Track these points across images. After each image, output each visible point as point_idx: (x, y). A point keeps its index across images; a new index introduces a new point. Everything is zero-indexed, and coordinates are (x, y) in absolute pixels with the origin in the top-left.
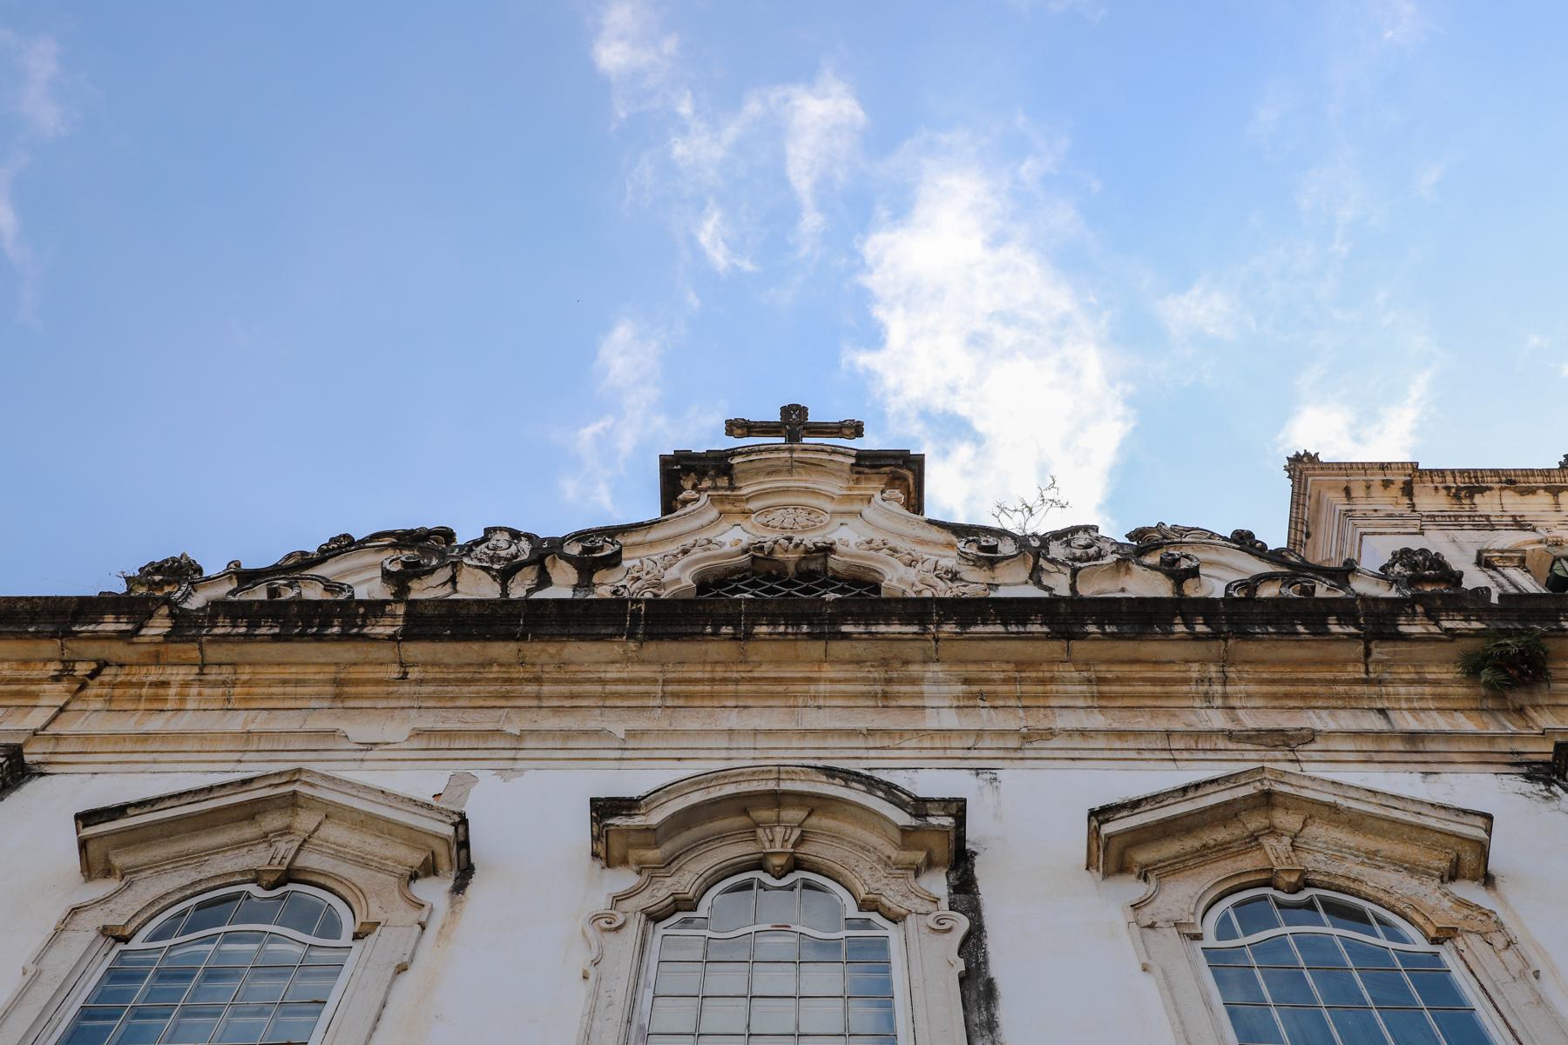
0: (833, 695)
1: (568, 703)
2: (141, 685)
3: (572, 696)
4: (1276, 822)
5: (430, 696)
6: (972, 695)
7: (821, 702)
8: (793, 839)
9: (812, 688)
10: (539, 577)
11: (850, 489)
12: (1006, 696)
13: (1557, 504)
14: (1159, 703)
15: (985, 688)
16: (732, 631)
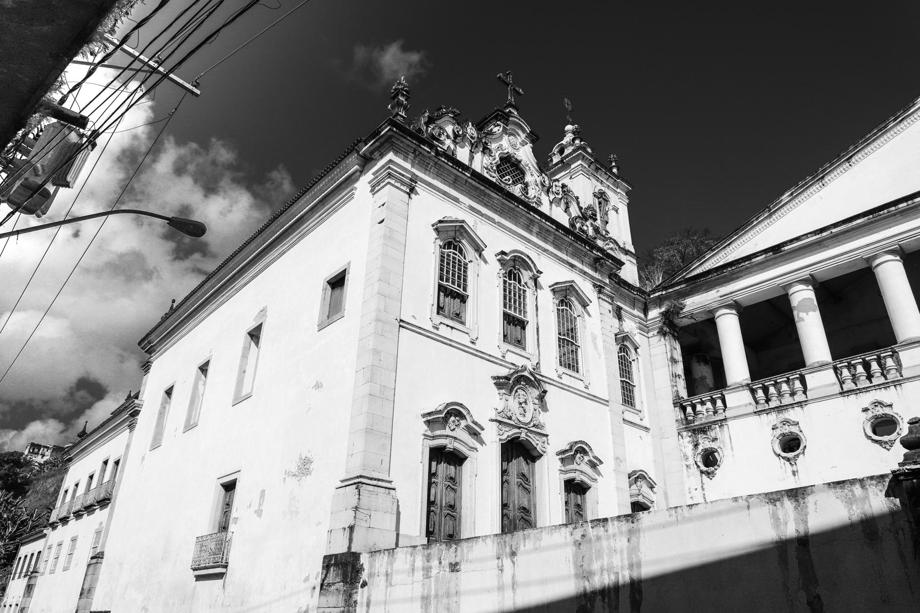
3: (488, 202)
5: (467, 190)
13: (608, 179)
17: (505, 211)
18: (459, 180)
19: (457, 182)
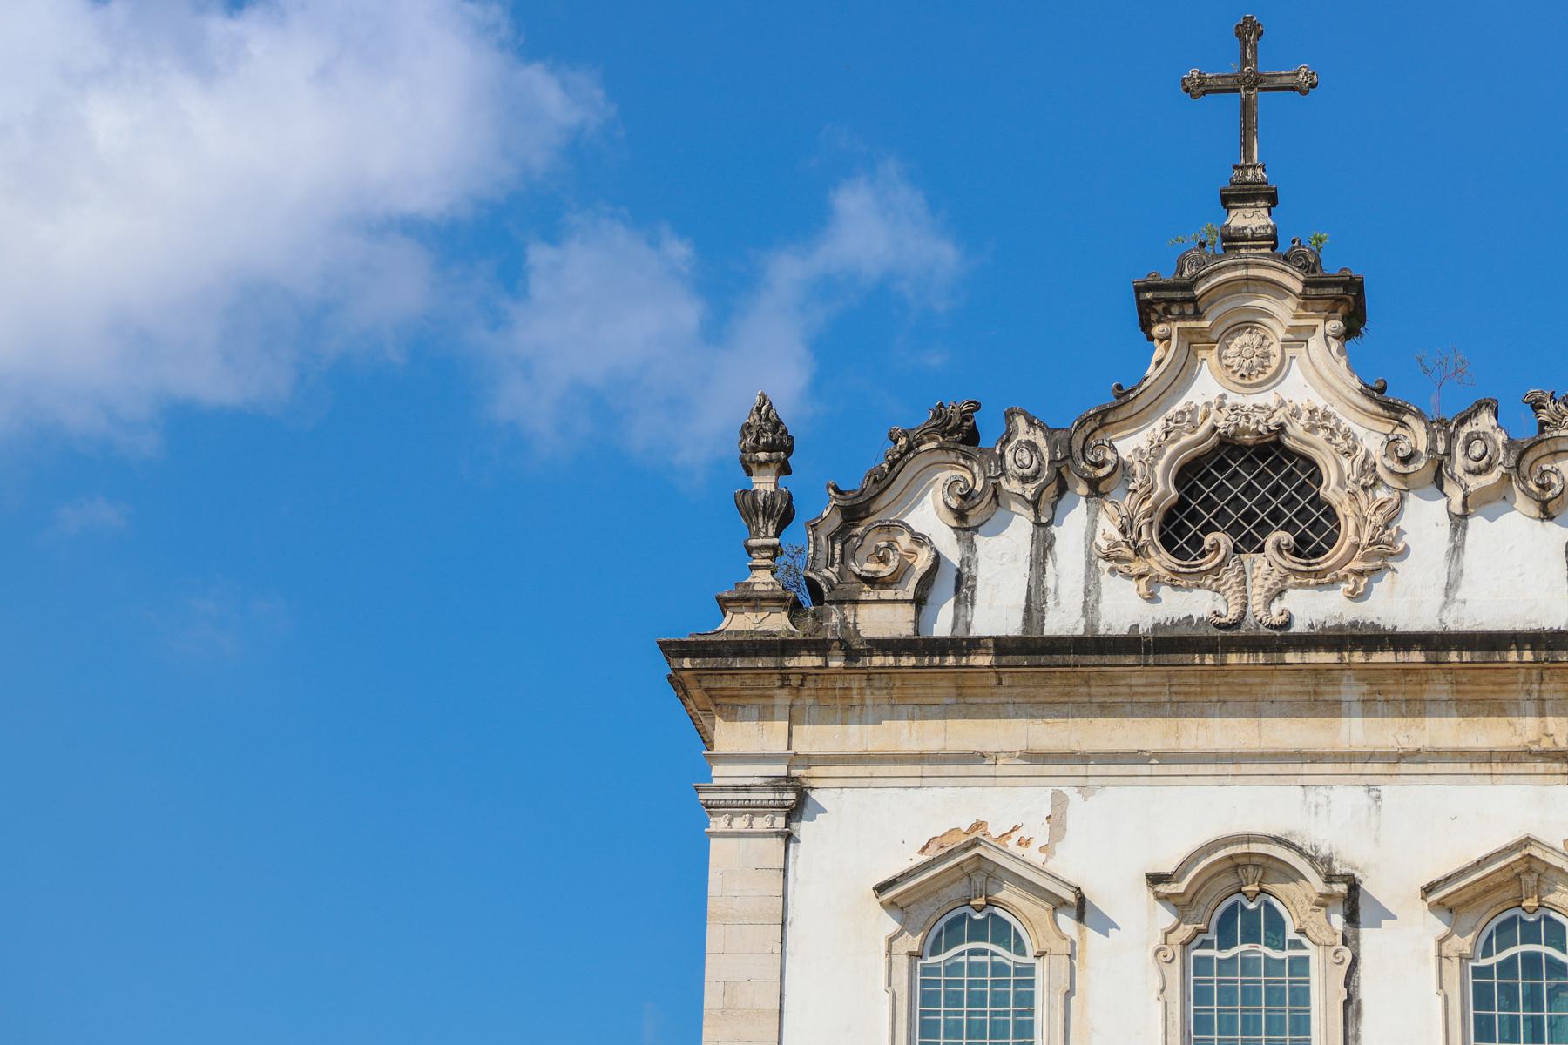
0: (1281, 693)
1: (1108, 699)
2: (834, 689)
3: (1111, 694)
4: (1532, 865)
6: (1373, 693)
7: (1274, 698)
8: (1259, 877)
9: (1267, 688)
10: (1058, 487)
11: (1298, 317)
12: (1396, 693)
14: (1494, 696)
15: (1381, 688)
16: (1212, 662)
17: (1193, 689)
18: (968, 683)
19: (965, 691)
